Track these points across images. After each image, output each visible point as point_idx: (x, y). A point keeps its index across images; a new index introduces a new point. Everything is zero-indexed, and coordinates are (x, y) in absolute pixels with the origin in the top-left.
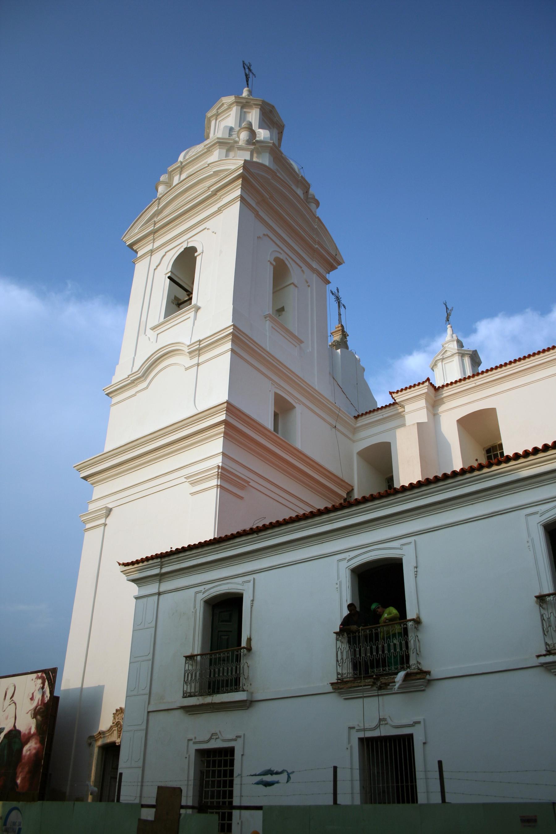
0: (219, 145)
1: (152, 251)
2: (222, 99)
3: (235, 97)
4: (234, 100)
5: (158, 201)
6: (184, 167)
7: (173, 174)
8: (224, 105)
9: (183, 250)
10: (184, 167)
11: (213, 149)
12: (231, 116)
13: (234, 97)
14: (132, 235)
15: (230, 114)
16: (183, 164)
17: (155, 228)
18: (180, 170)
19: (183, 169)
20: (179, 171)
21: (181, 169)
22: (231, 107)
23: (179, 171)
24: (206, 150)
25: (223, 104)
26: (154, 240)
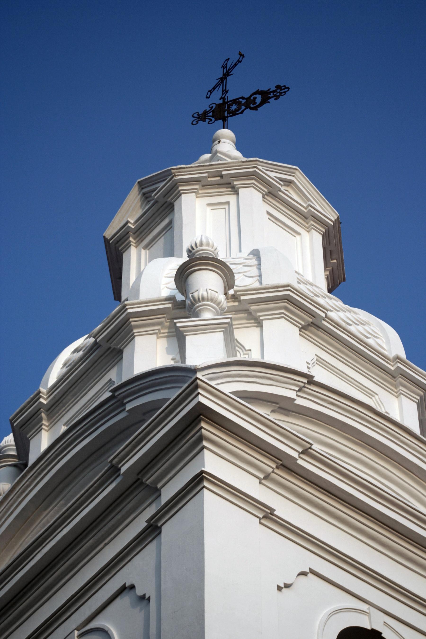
0: (421, 397)
1: (271, 514)
2: (297, 172)
3: (338, 218)
4: (331, 220)
5: (305, 381)
6: (319, 327)
7: (286, 308)
8: (288, 186)
9: (369, 628)
10: (319, 327)
11: (404, 386)
12: (298, 237)
13: (336, 217)
14: (212, 383)
15: (299, 234)
16: (324, 322)
17: (300, 462)
18: (307, 324)
19: (312, 329)
20: (303, 323)
21: (309, 325)
22: (312, 223)
23: (303, 323)
24: (393, 368)
25: (288, 183)
26: (267, 477)
